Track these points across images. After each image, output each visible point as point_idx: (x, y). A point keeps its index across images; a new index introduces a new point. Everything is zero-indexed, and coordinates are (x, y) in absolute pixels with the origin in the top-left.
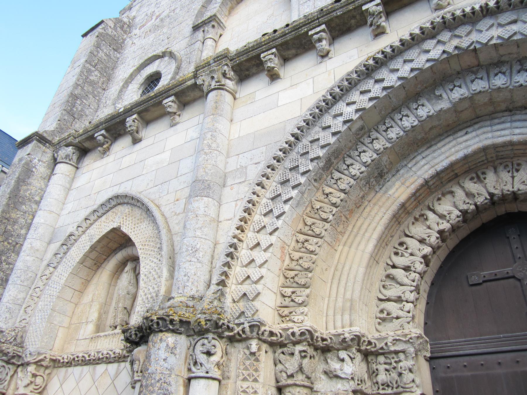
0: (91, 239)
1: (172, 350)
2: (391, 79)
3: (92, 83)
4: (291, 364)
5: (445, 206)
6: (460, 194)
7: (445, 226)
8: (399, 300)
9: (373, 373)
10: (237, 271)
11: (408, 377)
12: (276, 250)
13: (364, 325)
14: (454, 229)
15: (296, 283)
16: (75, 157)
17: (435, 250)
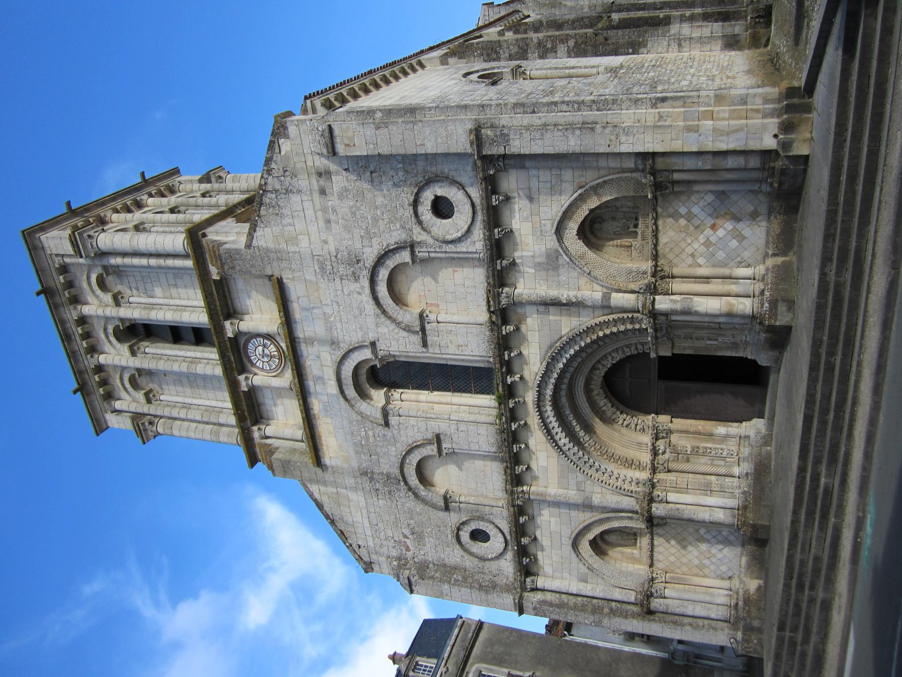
0: (592, 556)
1: (657, 508)
2: (556, 424)
3: (465, 579)
4: (661, 467)
5: (602, 403)
6: (597, 397)
7: (610, 405)
8: (636, 425)
9: (663, 438)
10: (626, 486)
11: (665, 427)
12: (619, 471)
13: (647, 439)
14: (610, 401)
15: (630, 463)
16: (532, 578)
17: (618, 409)
